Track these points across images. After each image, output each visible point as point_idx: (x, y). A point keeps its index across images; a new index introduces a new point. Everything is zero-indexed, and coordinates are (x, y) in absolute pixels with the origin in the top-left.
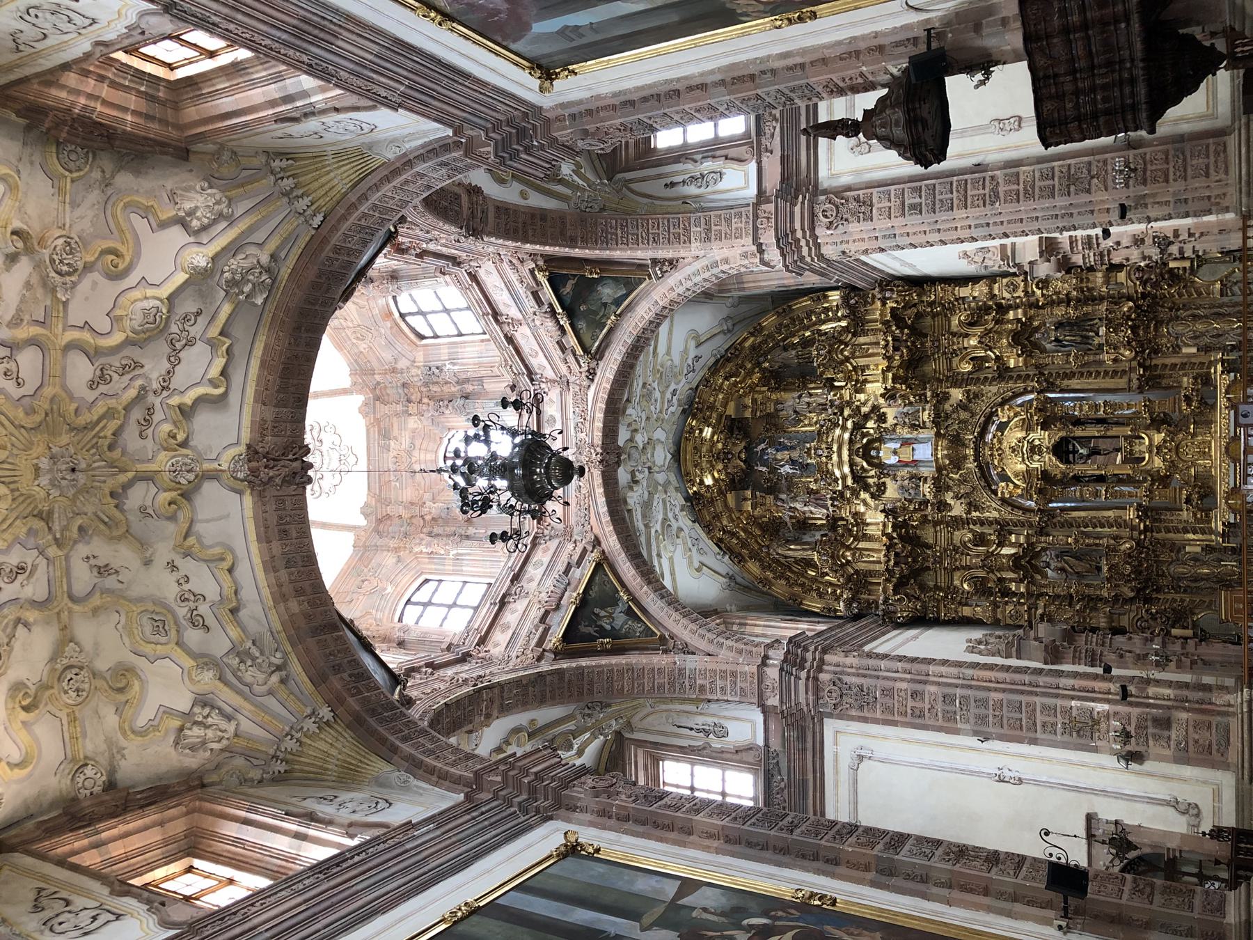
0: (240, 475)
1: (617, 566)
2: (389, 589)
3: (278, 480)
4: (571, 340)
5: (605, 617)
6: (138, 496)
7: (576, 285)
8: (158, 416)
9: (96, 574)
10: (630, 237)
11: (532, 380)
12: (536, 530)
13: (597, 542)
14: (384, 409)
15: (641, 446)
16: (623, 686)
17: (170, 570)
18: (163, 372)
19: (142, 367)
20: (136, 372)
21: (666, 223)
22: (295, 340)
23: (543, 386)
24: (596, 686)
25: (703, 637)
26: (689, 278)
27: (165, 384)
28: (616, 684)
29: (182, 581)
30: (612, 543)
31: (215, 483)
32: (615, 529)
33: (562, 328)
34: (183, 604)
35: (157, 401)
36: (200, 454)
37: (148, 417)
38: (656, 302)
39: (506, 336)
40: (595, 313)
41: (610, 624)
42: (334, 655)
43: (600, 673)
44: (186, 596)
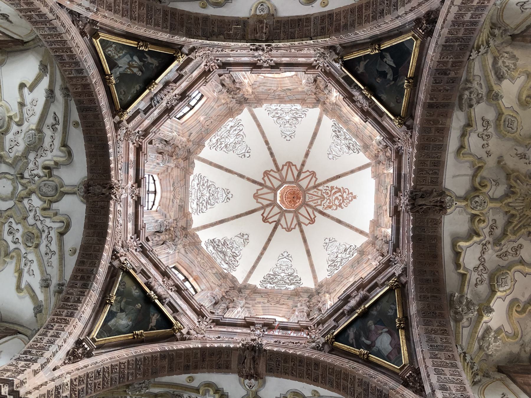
0: (449, 198)
1: (107, 104)
2: (202, 118)
3: (435, 194)
4: (141, 280)
5: (135, 67)
6: (499, 191)
7: (149, 323)
8: (486, 231)
9: (526, 155)
10: (118, 369)
11: (142, 247)
12: (143, 141)
13: (117, 126)
14: (182, 223)
15: (34, 197)
16: (139, 8)
17: (491, 152)
18: (486, 253)
19: (497, 256)
20: (499, 253)
21: (89, 391)
22: (434, 274)
23: (135, 243)
24: (161, 16)
25: (63, 25)
26: (60, 347)
27: (484, 247)
28: (145, 11)
29: (486, 146)
30: (109, 123)
31: (458, 195)
32: (107, 135)
33: (151, 288)
34: (489, 133)
35: (488, 238)
36: (465, 210)
37: (492, 230)
38: (79, 320)
39: (169, 277)
40: (128, 303)
41: (133, 60)
42: (445, 89)
43: (157, 25)
44: (486, 137)
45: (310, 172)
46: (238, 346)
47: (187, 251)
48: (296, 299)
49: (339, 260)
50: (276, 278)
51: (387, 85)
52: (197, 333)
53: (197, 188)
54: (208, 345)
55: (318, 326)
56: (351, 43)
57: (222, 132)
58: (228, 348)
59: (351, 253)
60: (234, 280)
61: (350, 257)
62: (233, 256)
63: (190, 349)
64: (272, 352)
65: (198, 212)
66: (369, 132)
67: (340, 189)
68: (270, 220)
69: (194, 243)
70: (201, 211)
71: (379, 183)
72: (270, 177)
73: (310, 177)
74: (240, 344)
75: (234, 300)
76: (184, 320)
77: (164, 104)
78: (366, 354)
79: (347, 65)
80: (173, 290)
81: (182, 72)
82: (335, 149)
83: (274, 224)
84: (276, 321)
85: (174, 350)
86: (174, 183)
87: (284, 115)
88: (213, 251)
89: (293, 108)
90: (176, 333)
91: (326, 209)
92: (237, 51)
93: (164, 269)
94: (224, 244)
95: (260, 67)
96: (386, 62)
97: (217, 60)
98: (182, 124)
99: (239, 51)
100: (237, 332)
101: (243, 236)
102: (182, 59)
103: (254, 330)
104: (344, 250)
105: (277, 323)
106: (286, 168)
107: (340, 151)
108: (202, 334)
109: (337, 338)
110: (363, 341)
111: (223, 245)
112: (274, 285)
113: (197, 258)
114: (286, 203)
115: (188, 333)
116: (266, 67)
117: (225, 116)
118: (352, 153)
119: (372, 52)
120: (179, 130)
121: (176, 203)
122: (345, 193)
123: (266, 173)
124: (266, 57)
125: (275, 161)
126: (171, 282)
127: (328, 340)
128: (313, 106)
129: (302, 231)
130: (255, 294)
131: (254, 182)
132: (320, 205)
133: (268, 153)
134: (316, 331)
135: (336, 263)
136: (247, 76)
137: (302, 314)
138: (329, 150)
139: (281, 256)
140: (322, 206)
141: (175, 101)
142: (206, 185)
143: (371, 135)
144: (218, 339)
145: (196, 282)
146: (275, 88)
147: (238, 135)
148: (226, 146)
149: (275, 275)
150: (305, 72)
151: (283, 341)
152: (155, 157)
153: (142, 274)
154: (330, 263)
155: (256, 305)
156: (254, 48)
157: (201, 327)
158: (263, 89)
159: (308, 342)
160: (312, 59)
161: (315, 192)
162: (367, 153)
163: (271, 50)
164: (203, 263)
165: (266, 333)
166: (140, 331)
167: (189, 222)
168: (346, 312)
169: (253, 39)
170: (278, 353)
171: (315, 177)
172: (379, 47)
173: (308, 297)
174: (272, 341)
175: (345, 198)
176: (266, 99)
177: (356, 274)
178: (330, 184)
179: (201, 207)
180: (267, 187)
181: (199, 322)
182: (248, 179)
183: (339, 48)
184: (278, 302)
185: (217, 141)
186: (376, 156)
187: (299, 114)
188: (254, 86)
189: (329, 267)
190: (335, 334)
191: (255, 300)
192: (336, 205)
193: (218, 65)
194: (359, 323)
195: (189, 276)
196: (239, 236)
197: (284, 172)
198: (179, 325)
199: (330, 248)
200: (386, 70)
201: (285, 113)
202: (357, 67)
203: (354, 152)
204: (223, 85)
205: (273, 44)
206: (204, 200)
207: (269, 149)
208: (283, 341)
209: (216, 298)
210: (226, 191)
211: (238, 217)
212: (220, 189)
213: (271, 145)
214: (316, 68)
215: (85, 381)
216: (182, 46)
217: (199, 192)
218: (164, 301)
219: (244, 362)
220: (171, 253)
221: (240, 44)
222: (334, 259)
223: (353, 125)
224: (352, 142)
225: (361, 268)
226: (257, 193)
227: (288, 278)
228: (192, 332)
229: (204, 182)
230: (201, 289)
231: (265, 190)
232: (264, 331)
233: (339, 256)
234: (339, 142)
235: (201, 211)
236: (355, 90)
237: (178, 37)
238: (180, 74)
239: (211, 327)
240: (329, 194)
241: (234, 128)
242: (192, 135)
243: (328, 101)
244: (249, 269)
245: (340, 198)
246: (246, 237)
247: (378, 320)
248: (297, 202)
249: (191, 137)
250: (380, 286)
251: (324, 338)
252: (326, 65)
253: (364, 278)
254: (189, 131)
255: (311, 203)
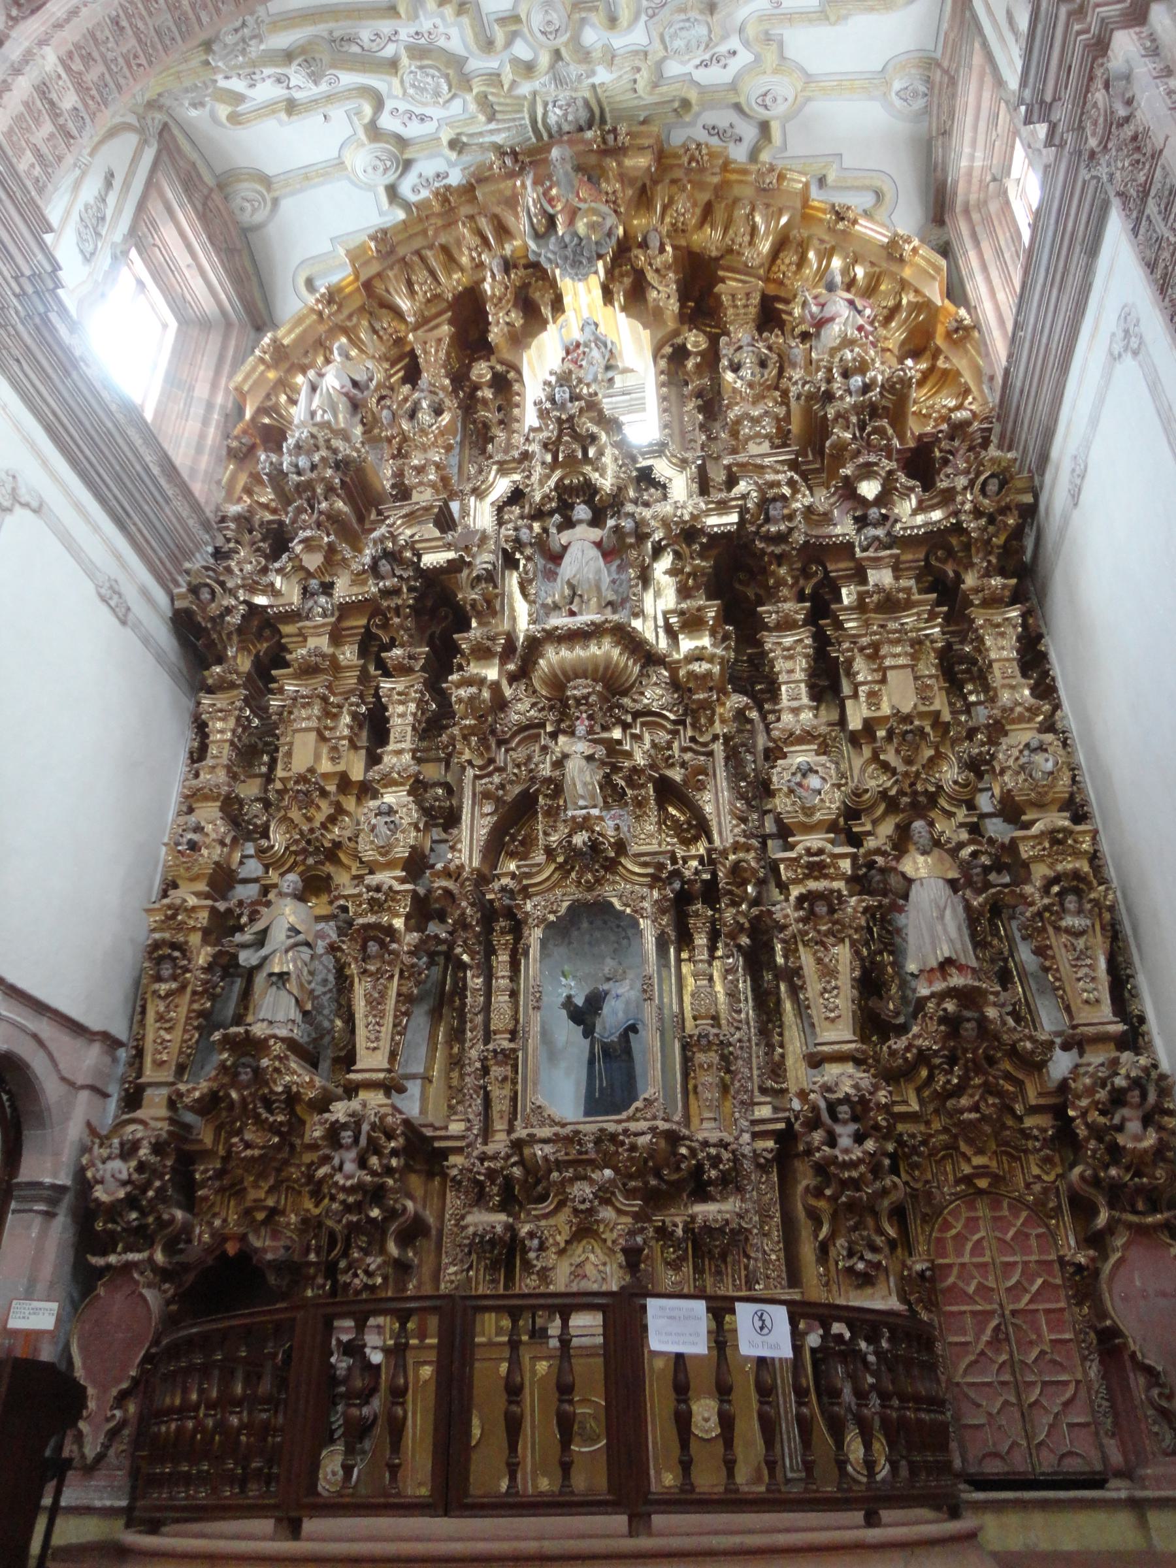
21: (122, 81)
215: (96, 55)
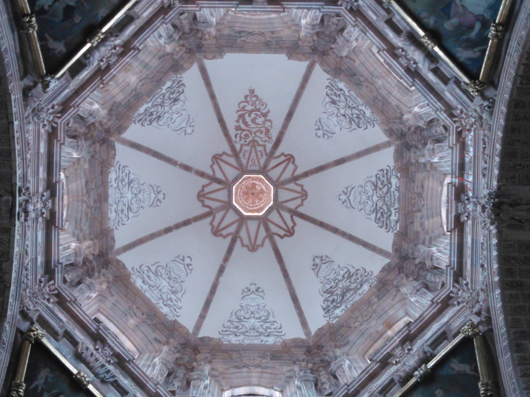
2: (132, 322)
7: (464, 375)
14: (300, 354)
33: (409, 376)
39: (390, 355)
45: (213, 164)
46: (494, 231)
47: (347, 341)
48: (412, 169)
49: (349, 112)
50: (381, 208)
51: (84, 6)
52: (478, 302)
53: (242, 337)
54: (496, 279)
55: (455, 117)
56: (20, 63)
57: (152, 297)
58: (500, 246)
59: (338, 93)
60: (387, 269)
61: (344, 94)
62: (349, 277)
63: (504, 307)
64: (501, 178)
65: (280, 334)
66: (154, 60)
67: (240, 116)
68: (290, 224)
69: (331, 334)
70: (280, 330)
71: (231, 47)
72: (222, 226)
73: (222, 164)
74: (492, 227)
75: (420, 263)
76: (456, 325)
77: (111, 368)
78: (495, 27)
79: (53, 70)
80: (410, 347)
81: (60, 331)
82: (177, 123)
83: (296, 219)
84: (451, 183)
85: (508, 331)
86: (236, 367)
87: (125, 200)
88: (343, 307)
89: (115, 185)
90: (480, 332)
91: (270, 138)
92: (27, 246)
93: (376, 364)
94: (330, 292)
95: (53, 213)
96: (50, 6)
97: (41, 282)
98: (140, 353)
99: (27, 243)
100: (472, 240)
101: (317, 265)
102: (39, 331)
103: (466, 214)
104: (333, 105)
105: (454, 180)
106: (207, 202)
107: (182, 114)
108: (478, 295)
109: (473, 76)
110: (477, 34)
111: (332, 295)
112: (392, 209)
113: (355, 327)
114: (262, 205)
115: (478, 314)
116: (53, 203)
117: (127, 287)
118: (184, 96)
119: (34, 28)
120: (149, 357)
121: (267, 363)
122: (246, 108)
123: (216, 232)
124: (38, 201)
125: (197, 219)
126: (398, 352)
127: (478, 91)
128: (112, 149)
129: (306, 174)
130: (409, 234)
131: (230, 251)
132: (264, 146)
133: (183, 229)
134: (463, 118)
135: (355, 116)
136: (65, 244)
137: (437, 151)
138: (179, 132)
139: (345, 204)
140: (267, 143)
141: (105, 350)
142: (236, 324)
143: (157, 57)
144: (486, 266)
145: (394, 324)
146: (85, 206)
147: (156, 274)
148: (174, 292)
149: (376, 211)
150: (61, 144)
151: (482, 164)
152: (195, 389)
153: (387, 392)
154: (354, 126)
155: (426, 228)
156: (23, 214)
157: (467, 298)
158: (85, 225)
159: (481, 126)
160: (42, 131)
161: (244, 155)
162: (185, 66)
163: (28, 189)
164: (362, 317)
165: (471, 194)
166: (480, 386)
167: (297, 343)
168: (433, 66)
169: (9, 214)
170: (502, 167)
171: (221, 155)
172: (27, 15)
173: (409, 150)
174: (483, 181)
175: (253, 108)
176: (101, 223)
177: (370, 76)
178: (232, 132)
179: (272, 330)
180: (238, 231)
181: (459, 303)
182: (226, 259)
183: (28, 82)
184: (420, 195)
185: (165, 305)
186: (189, 52)
187: (124, 177)
188: (81, 237)
189: (360, 126)
190: (466, 80)
191: (417, 234)
192: (264, 122)
193: (49, 281)
194: (448, 44)
195: (384, 336)
196: (316, 271)
197: (214, 205)
198: (466, 327)
199: (331, 127)
200: (62, 8)
201: (122, 199)
202: (56, 52)
203: (183, 92)
204: (79, 283)
205: (19, 184)
206: (262, 326)
207: (178, 226)
208: (482, 164)
209: (418, 288)
210: (245, 294)
211: (286, 275)
212: (243, 302)
213: (171, 224)
214: (56, 126)
216: (19, 331)
217: (247, 334)
218: (429, 354)
219: (520, 221)
220: (349, 362)
221: (17, 237)
222: (348, 120)
223: (143, 85)
224: (167, 95)
225: (361, 69)
226: (247, 246)
227: (381, 189)
228: (475, 310)
229: (231, 326)
230: (404, 316)
231: (243, 234)
232: (468, 199)
233: (342, 111)
234: (166, 115)
235: (280, 330)
236: (92, 59)
237: (4, 334)
238: (64, 336)
239: (467, 284)
240: (247, 132)
241: (146, 278)
242: (158, 337)
243: (105, 121)
244: (369, 253)
245: (253, 116)
246: (318, 261)
247: (442, 13)
248: (259, 188)
249: (162, 340)
250: (390, 16)
251: (474, 97)
252: (51, 111)
253: (379, 48)
254: (153, 341)
255: (262, 161)
